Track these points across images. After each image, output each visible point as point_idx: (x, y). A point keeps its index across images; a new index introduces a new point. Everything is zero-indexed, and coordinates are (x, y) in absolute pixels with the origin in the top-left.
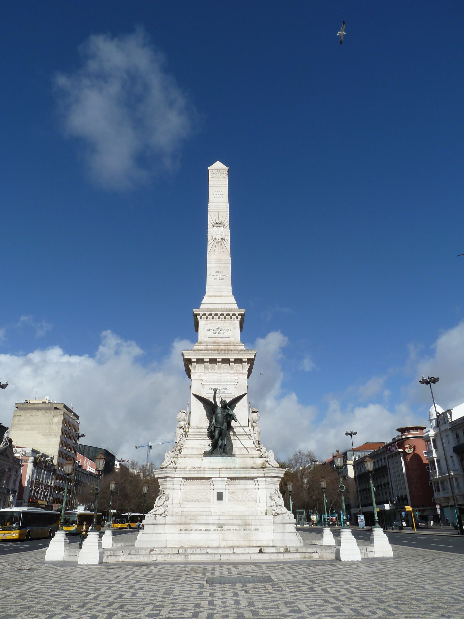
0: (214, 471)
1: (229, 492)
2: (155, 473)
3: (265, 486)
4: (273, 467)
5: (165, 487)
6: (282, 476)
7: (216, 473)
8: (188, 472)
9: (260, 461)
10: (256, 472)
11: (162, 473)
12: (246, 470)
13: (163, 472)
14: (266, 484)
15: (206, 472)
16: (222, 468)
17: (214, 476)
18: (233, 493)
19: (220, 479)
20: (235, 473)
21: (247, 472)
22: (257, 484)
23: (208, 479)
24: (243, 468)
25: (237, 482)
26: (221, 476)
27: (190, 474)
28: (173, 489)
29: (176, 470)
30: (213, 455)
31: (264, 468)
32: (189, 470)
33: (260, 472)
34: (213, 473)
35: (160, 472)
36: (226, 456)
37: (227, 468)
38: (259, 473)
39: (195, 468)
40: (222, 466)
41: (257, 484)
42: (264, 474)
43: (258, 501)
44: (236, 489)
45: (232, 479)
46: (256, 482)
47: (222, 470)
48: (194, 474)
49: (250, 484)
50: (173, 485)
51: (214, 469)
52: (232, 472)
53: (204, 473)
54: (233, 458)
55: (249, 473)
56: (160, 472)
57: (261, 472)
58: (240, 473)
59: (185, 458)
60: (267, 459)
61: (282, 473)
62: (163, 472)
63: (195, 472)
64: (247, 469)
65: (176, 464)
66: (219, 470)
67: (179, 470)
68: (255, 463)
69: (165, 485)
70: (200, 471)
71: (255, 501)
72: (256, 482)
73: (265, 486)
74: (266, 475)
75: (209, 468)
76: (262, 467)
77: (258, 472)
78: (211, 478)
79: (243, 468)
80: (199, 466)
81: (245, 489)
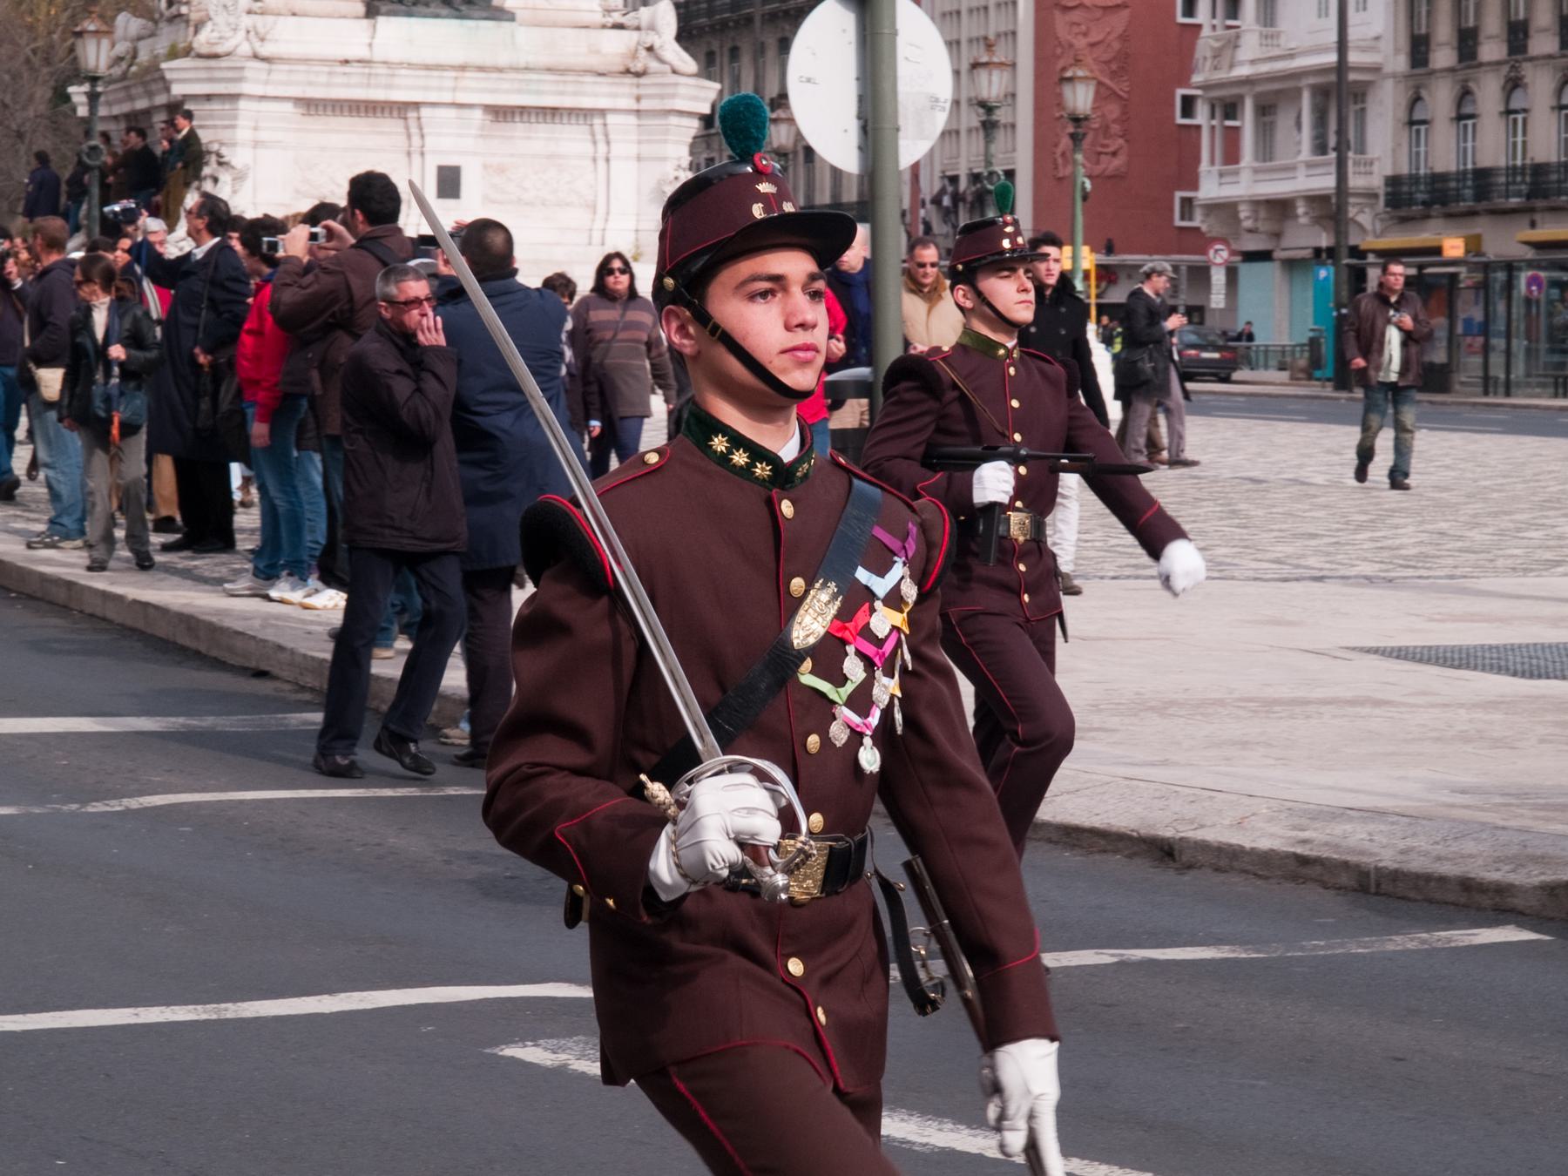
0: (434, 78)
1: (485, 167)
2: (168, 76)
3: (633, 150)
4: (674, 72)
5: (224, 135)
6: (706, 110)
7: (440, 89)
8: (323, 79)
9: (616, 45)
10: (606, 89)
11: (211, 80)
12: (565, 82)
13: (218, 74)
14: (639, 142)
15: (397, 81)
16: (463, 68)
17: (433, 98)
18: (501, 170)
19: (452, 112)
20: (519, 91)
21: (570, 88)
22: (600, 137)
23: (401, 109)
24: (549, 70)
25: (519, 128)
26: (462, 98)
27: (328, 85)
28: (256, 144)
29: (274, 67)
30: (420, 9)
31: (638, 75)
32: (326, 69)
33: (621, 90)
34: (426, 88)
35: (203, 75)
36: (477, 14)
37: (481, 69)
38: (615, 95)
39: (347, 62)
40: (458, 58)
41: (600, 137)
42: (638, 99)
43: (601, 210)
44: (512, 155)
45: (501, 113)
46: (598, 128)
47: (468, 74)
48: (347, 85)
49: (571, 140)
50: (256, 129)
51: (428, 67)
52: (506, 86)
53: (389, 87)
54: (506, 25)
55: (575, 94)
56: (203, 75)
57: (626, 90)
58: (539, 93)
59: (294, 14)
60: (651, 38)
61: (704, 100)
62: (218, 74)
63: (354, 80)
64: (570, 78)
65: (262, 40)
66: (453, 74)
67: (286, 67)
68: (598, 52)
69: (226, 127)
70: (377, 75)
71: (593, 208)
72: (598, 128)
73: (633, 150)
74: (645, 105)
75: (410, 66)
76: (628, 72)
77: (614, 89)
78: (416, 105)
79: (549, 70)
80: (363, 53)
81: (550, 157)
